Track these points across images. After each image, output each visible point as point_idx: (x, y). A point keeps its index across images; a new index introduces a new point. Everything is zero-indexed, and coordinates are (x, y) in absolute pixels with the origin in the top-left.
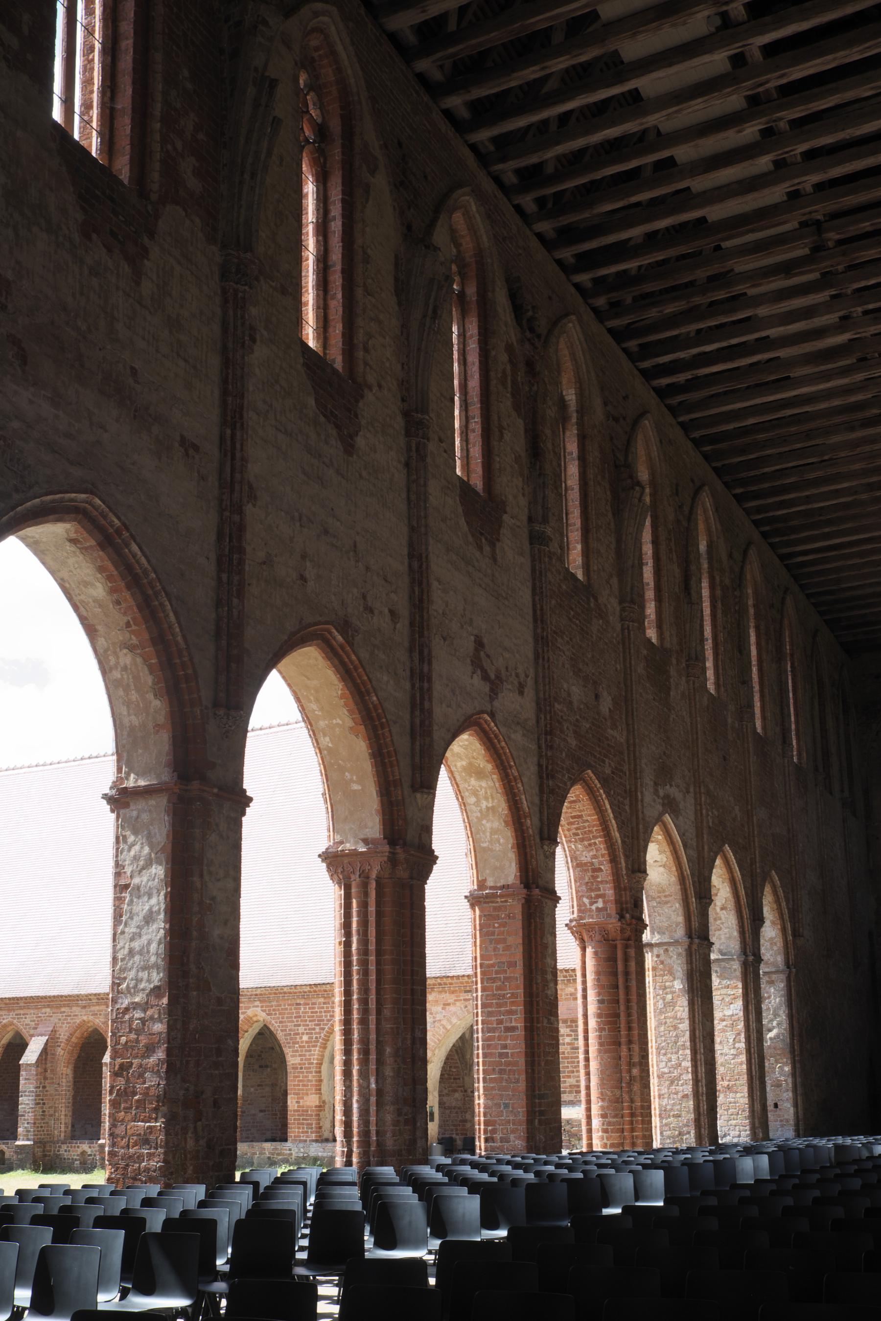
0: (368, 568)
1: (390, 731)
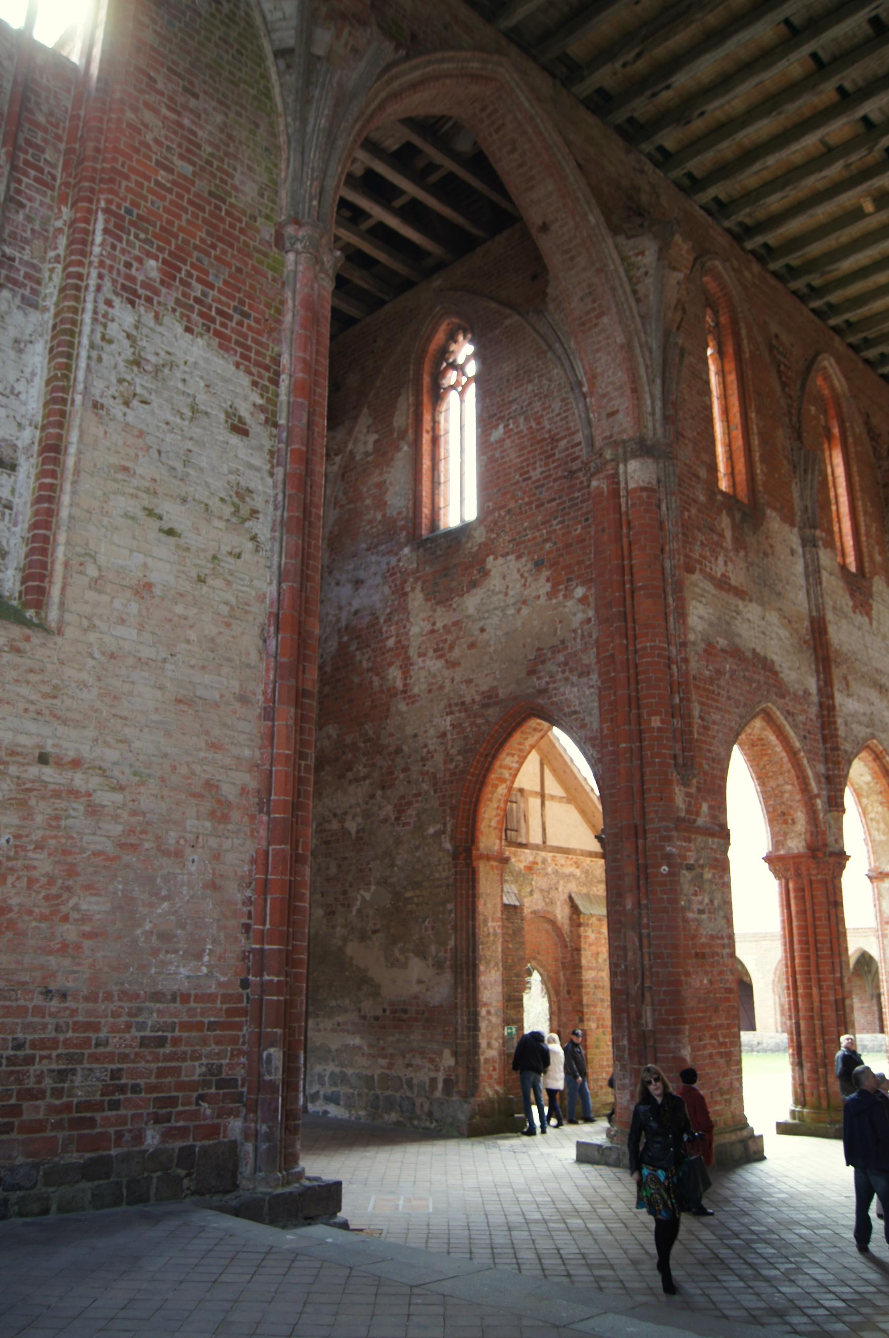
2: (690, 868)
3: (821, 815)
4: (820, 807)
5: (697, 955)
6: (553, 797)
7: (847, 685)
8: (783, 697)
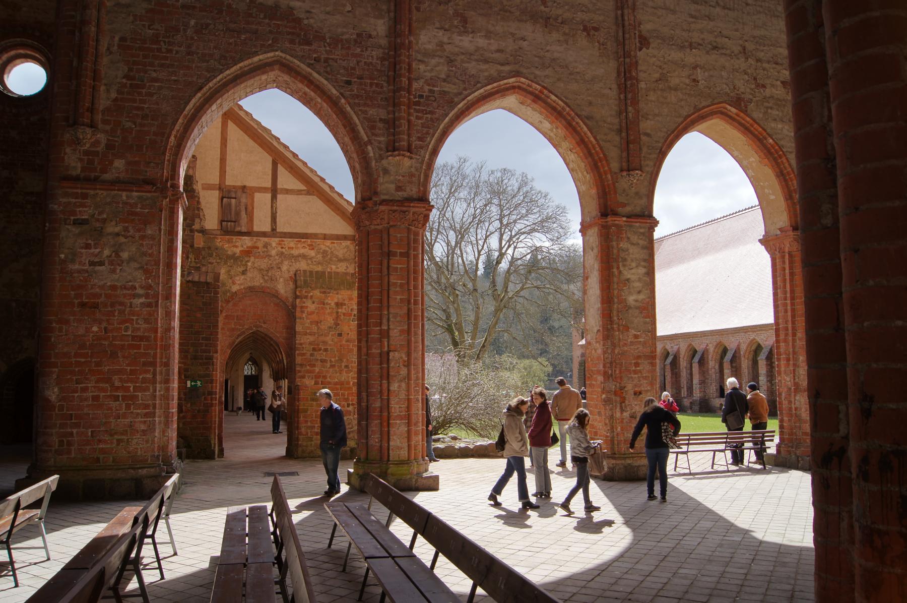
0: (758, 60)
1: (787, 159)
2: (76, 223)
3: (373, 163)
4: (371, 154)
5: (83, 305)
6: (287, 191)
7: (465, 21)
8: (309, 43)
